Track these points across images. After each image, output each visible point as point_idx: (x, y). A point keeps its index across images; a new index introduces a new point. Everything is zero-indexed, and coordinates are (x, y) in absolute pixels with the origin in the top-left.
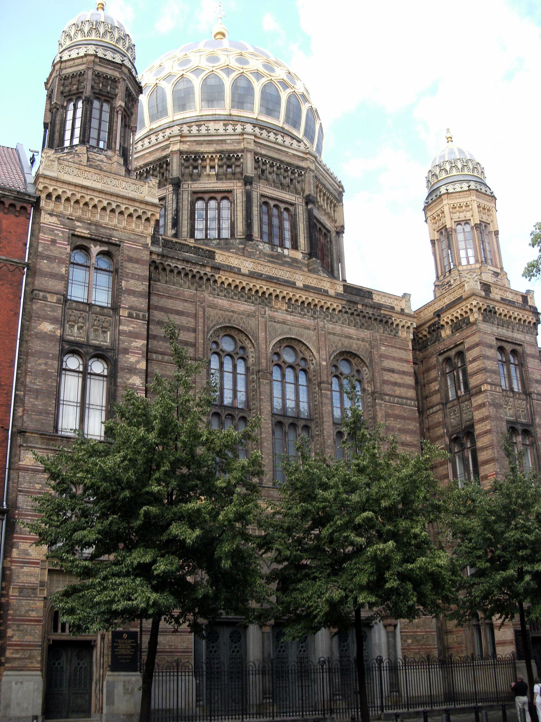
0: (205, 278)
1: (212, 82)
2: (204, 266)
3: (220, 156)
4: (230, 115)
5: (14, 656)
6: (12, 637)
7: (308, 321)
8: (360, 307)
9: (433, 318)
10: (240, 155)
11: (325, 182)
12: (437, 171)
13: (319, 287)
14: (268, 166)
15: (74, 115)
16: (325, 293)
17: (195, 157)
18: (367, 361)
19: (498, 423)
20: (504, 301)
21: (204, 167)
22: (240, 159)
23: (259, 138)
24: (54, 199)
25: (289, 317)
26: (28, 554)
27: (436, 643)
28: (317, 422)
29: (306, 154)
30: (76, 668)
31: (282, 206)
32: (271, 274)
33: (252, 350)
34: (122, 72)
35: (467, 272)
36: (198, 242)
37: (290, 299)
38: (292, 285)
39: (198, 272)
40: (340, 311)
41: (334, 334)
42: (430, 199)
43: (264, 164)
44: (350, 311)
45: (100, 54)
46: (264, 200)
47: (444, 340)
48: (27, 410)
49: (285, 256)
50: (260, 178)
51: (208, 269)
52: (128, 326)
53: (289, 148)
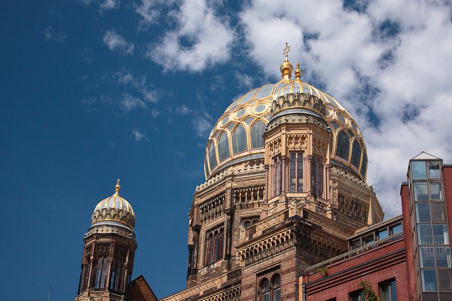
12: (281, 102)
42: (269, 127)
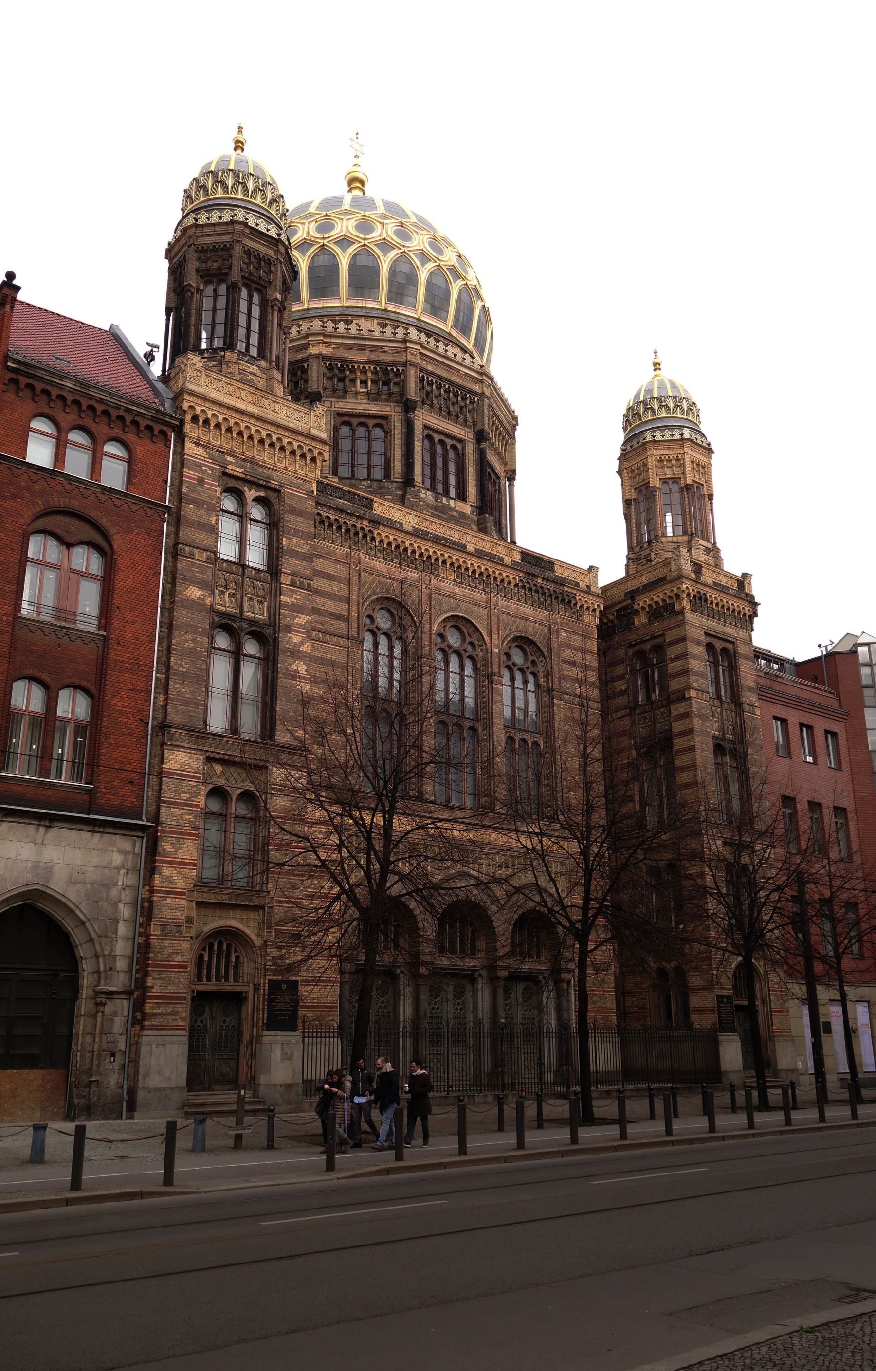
0: (361, 534)
1: (363, 261)
2: (361, 518)
3: (375, 368)
4: (386, 310)
5: (154, 1011)
6: (153, 987)
7: (479, 595)
8: (540, 581)
9: (624, 601)
10: (401, 369)
11: (499, 413)
14: (434, 387)
15: (209, 302)
16: (499, 561)
18: (545, 650)
19: (704, 738)
20: (717, 586)
21: (353, 381)
22: (399, 375)
23: (425, 348)
24: (201, 423)
25: (457, 590)
26: (173, 882)
27: (615, 1006)
28: (485, 724)
29: (481, 374)
30: (221, 1026)
31: (449, 442)
34: (277, 251)
35: (673, 545)
36: (344, 481)
37: (459, 567)
38: (461, 548)
39: (354, 526)
40: (516, 585)
41: (508, 614)
43: (430, 384)
45: (251, 223)
46: (427, 432)
47: (637, 629)
48: (172, 700)
49: (451, 509)
50: (423, 403)
51: (366, 523)
52: (290, 597)
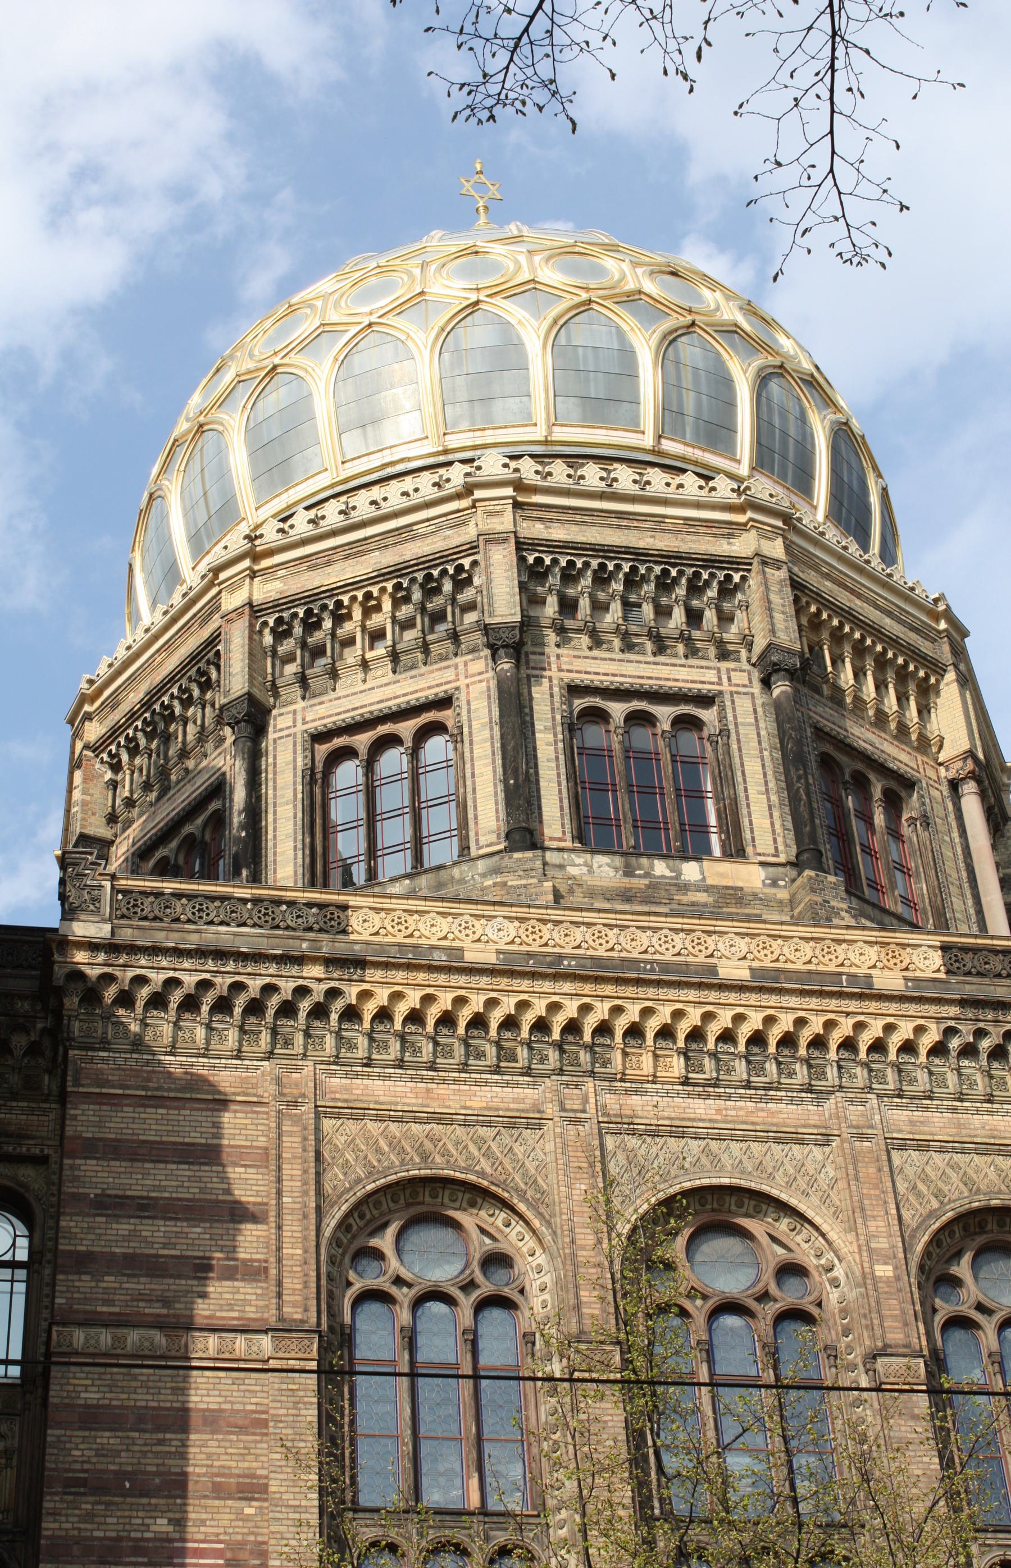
2: (300, 960)
3: (398, 587)
10: (466, 562)
11: (857, 604)
13: (832, 968)
17: (309, 612)
22: (469, 581)
23: (535, 490)
25: (701, 1109)
29: (740, 509)
31: (664, 713)
32: (601, 952)
33: (541, 1259)
38: (706, 980)
41: (922, 1146)
44: (985, 1044)
46: (580, 703)
49: (685, 888)
53: (665, 502)
